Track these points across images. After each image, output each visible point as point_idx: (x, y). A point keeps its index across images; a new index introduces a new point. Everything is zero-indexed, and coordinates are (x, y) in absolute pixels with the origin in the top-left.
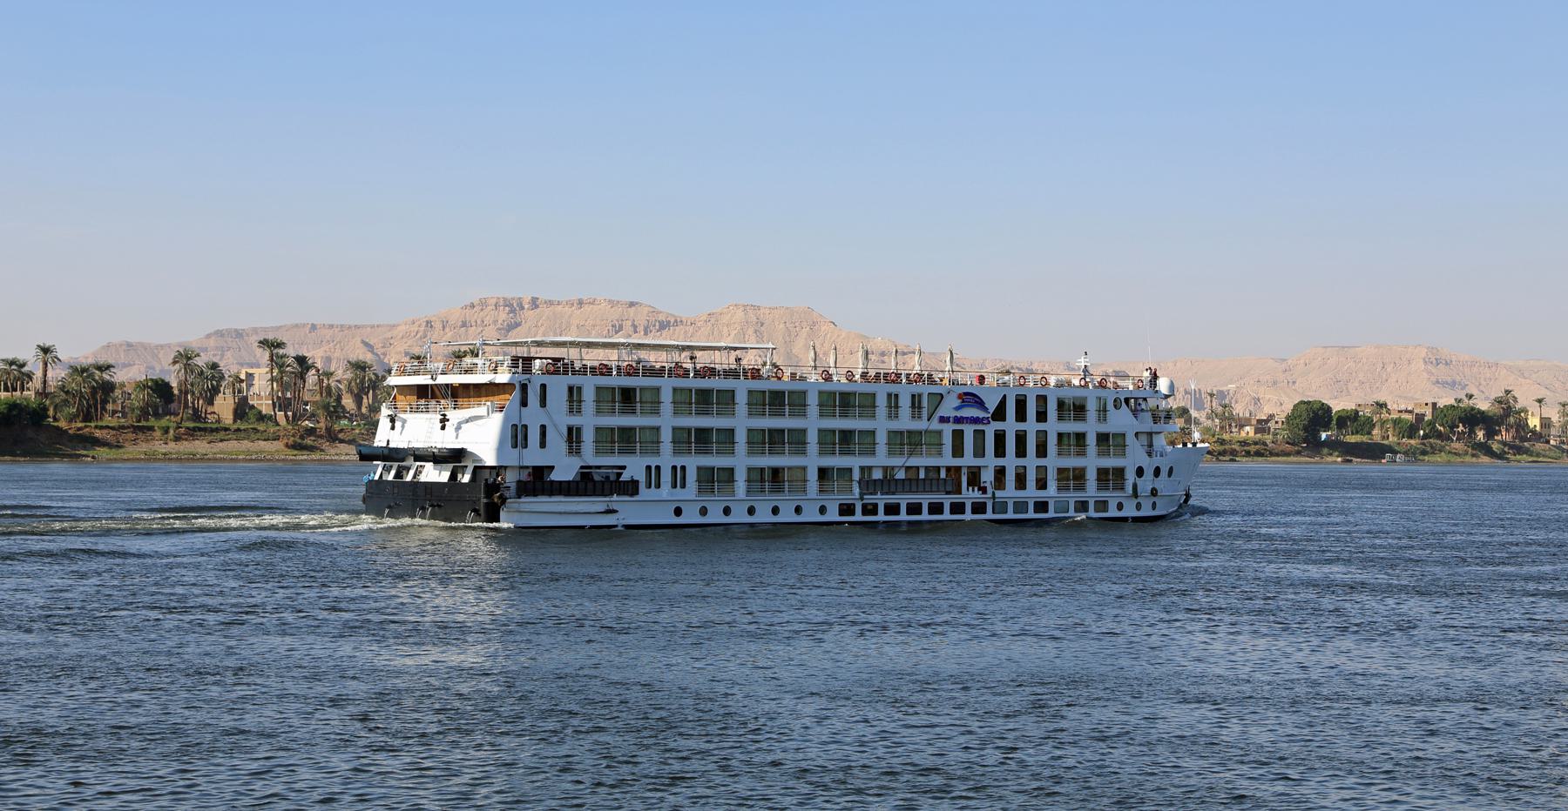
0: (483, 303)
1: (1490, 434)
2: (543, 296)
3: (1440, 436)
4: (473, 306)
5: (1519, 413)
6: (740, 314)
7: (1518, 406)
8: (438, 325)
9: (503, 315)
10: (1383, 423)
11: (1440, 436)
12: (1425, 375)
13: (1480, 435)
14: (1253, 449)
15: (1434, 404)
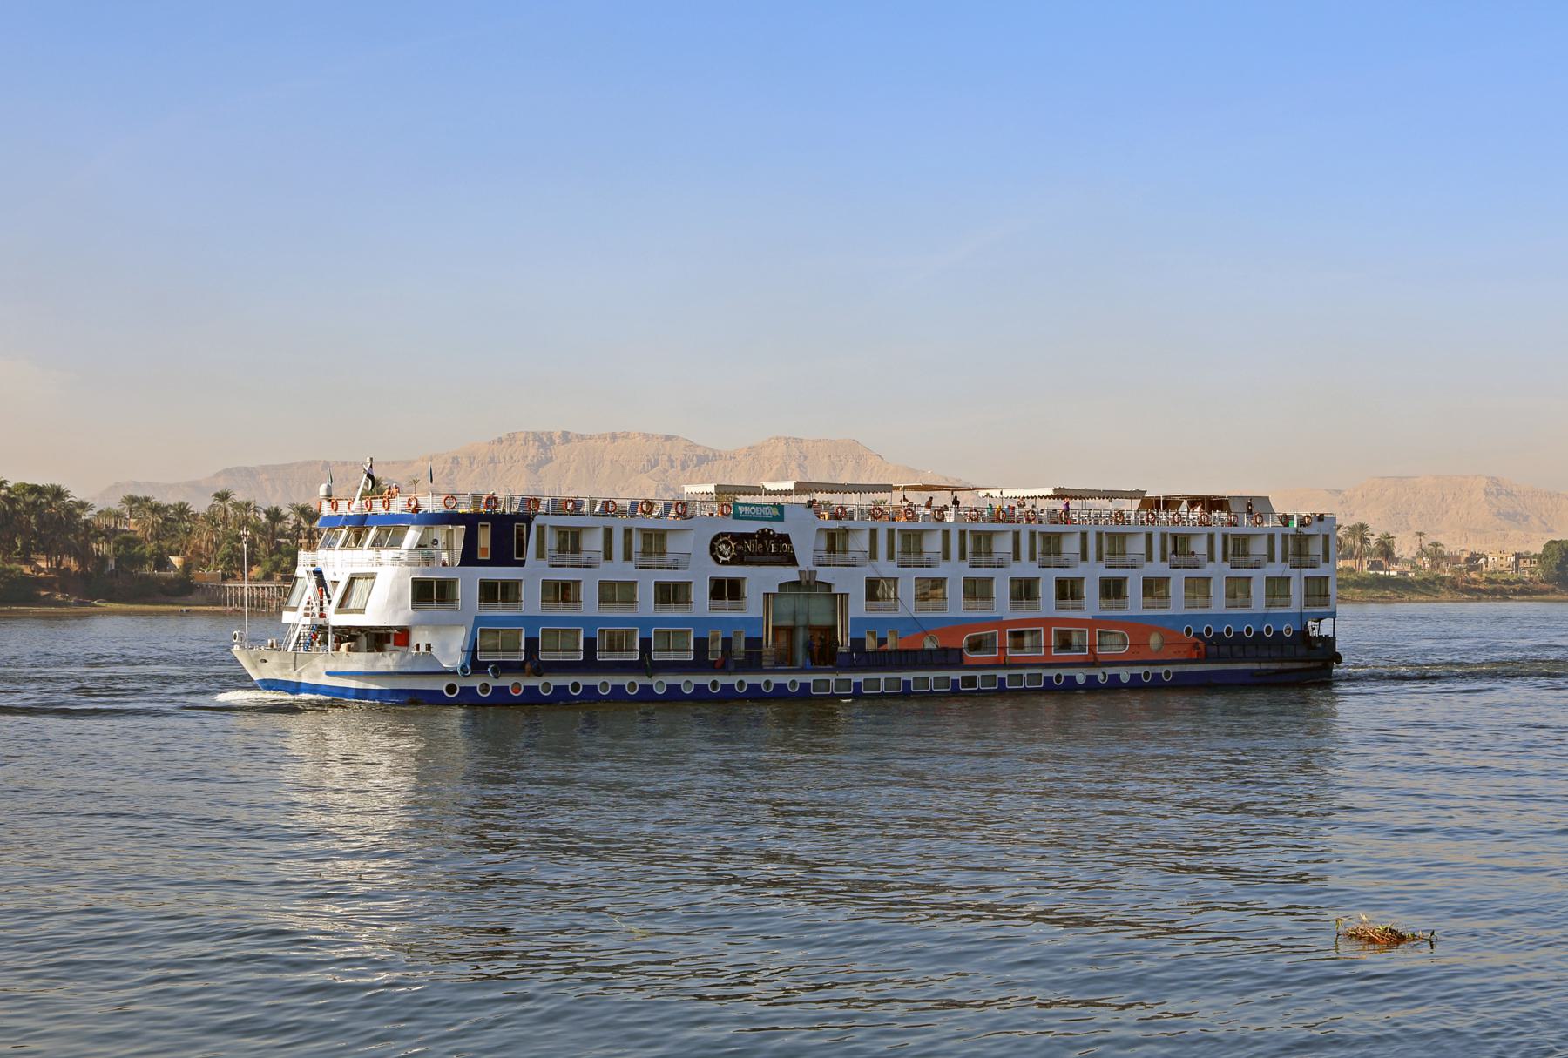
0: (512, 438)
2: (574, 429)
4: (500, 441)
6: (782, 447)
8: (465, 462)
9: (533, 450)
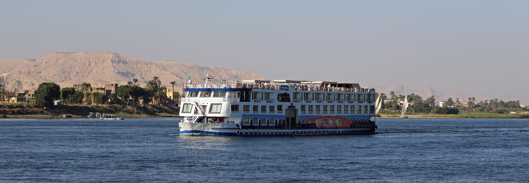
1: (146, 101)
3: (119, 102)
5: (162, 89)
7: (161, 86)
10: (88, 95)
11: (119, 102)
12: (112, 69)
13: (141, 101)
14: (16, 110)
15: (116, 85)
